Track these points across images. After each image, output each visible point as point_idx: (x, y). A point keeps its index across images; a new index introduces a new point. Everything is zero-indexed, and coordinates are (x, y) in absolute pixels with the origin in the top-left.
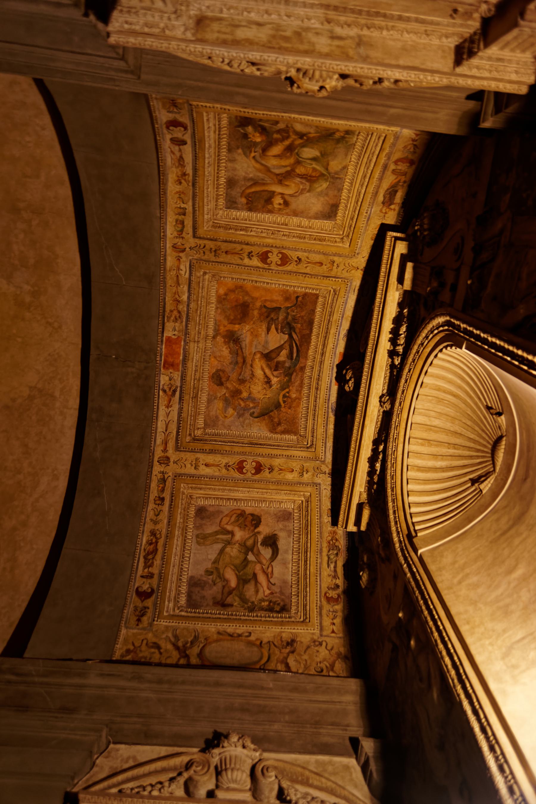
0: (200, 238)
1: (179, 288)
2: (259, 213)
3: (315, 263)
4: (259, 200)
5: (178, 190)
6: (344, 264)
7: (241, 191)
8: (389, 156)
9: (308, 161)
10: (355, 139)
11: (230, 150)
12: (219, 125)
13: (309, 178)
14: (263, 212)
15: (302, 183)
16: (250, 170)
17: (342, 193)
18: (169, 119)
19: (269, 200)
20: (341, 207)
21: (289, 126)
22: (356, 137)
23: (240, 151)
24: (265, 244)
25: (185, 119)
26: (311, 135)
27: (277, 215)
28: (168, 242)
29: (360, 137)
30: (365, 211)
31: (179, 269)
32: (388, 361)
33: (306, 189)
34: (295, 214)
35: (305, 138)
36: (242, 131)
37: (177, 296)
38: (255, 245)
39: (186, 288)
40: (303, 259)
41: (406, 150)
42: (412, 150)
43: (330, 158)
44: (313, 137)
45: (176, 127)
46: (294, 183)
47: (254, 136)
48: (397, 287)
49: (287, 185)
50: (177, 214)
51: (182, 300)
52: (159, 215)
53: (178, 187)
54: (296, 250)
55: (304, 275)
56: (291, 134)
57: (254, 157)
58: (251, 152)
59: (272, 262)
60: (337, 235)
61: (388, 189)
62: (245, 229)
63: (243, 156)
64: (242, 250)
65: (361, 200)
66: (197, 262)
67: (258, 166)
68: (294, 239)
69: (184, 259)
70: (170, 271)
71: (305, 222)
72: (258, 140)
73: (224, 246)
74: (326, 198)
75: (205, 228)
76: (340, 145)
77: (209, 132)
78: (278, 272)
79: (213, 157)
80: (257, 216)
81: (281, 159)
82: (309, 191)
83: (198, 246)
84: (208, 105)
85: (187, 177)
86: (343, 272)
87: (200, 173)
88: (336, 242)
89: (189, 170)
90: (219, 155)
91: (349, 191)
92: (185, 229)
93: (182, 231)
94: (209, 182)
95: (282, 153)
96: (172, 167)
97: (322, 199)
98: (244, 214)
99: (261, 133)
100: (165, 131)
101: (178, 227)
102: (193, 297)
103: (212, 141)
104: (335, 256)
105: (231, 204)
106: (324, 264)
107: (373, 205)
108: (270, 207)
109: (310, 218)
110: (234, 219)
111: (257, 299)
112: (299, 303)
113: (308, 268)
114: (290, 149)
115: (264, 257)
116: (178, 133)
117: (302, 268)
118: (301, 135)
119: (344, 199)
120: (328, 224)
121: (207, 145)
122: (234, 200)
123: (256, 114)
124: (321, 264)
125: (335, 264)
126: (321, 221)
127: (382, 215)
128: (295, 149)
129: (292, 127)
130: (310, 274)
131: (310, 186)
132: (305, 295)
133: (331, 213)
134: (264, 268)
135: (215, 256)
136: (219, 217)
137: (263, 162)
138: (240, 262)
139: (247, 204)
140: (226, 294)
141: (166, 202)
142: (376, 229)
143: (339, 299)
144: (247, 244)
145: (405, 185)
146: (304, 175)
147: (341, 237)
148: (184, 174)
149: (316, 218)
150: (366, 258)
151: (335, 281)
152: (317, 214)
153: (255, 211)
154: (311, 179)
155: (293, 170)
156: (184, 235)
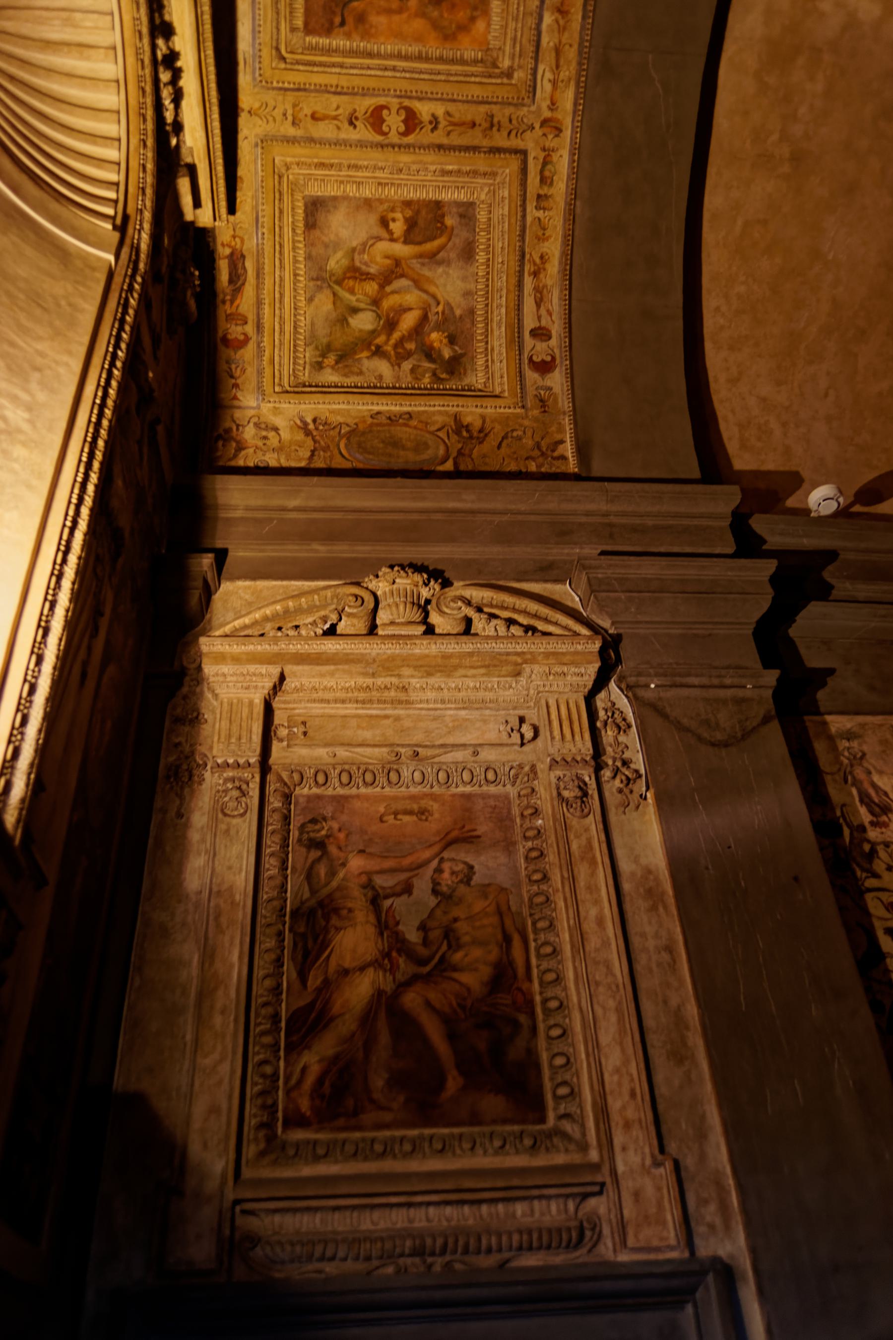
0: (516, 151)
1: (557, 41)
2: (424, 200)
3: (324, 118)
4: (426, 223)
5: (546, 244)
6: (275, 120)
7: (453, 239)
8: (260, 350)
9: (362, 306)
10: (307, 355)
11: (472, 312)
12: (487, 361)
13: (357, 274)
14: (419, 201)
15: (366, 264)
16: (442, 281)
17: (305, 252)
18: (550, 375)
19: (411, 224)
20: (301, 225)
21: (396, 368)
22: (307, 359)
23: (458, 312)
24: (412, 150)
25: (531, 376)
26: (365, 354)
27: (396, 197)
28: (569, 140)
29: (301, 362)
30: (266, 236)
31: (554, 83)
32: (170, 14)
33: (359, 254)
34: (368, 203)
35: (373, 348)
36: (457, 348)
37: (562, 22)
38: (429, 147)
39: (545, 39)
40: (346, 125)
41: (241, 366)
42: (233, 366)
43: (334, 315)
44: (362, 351)
45: (543, 361)
46: (377, 264)
47: (441, 341)
48: (193, 156)
49: (387, 257)
50: (550, 196)
51: (553, 13)
52: (578, 203)
53: (545, 250)
54: (361, 144)
55: (339, 89)
56: (392, 353)
57: (438, 304)
58: (443, 313)
59: (398, 113)
60: (299, 174)
61: (243, 284)
62: (444, 173)
63: (453, 304)
64: (449, 134)
65: (277, 255)
66: (523, 99)
67: (432, 289)
68: (366, 163)
69: (545, 105)
70: (570, 79)
71: (351, 190)
72: (434, 336)
73: (475, 138)
74: (326, 239)
75: (507, 171)
76: (325, 341)
77: (500, 354)
78: (385, 92)
79: (495, 305)
80: (428, 193)
81: (400, 305)
82: (354, 250)
83: (520, 133)
84: (502, 410)
85: (532, 269)
86: (274, 104)
87: (514, 281)
88: (298, 164)
89: (528, 282)
90: (487, 305)
91: (296, 261)
92: (539, 167)
93: (545, 163)
94: (500, 260)
95: (400, 315)
96: (552, 286)
97: (332, 237)
98: (446, 196)
99: (432, 348)
100: (557, 352)
101: (550, 171)
102: (531, 22)
103: (496, 333)
104: (295, 137)
105: (467, 212)
106: (309, 118)
107: (258, 251)
108: (409, 213)
109: (346, 198)
110: (463, 187)
111: (416, 15)
112: (338, 11)
113: (335, 106)
114: (391, 325)
115: (411, 121)
116: (540, 350)
117: (345, 105)
118: (379, 352)
119: (300, 242)
120: (315, 190)
121: (503, 329)
122: (463, 221)
123: (443, 406)
124: (314, 117)
125: (290, 118)
126: (326, 194)
127: (238, 232)
128: (384, 327)
129: (393, 366)
130: (329, 92)
131: (353, 260)
132: (328, 31)
133: (315, 208)
134: (410, 98)
135: (492, 116)
136: (486, 189)
137: (425, 296)
138: (451, 107)
139: (443, 216)
140: (473, 19)
141: (565, 220)
142: (241, 202)
143: (269, 36)
144: (440, 147)
145: (221, 296)
146: (365, 280)
147: (290, 171)
148: (535, 274)
149: (335, 199)
150: (241, 136)
151: (283, 83)
152: (335, 207)
153: (430, 201)
154: (355, 273)
155: (382, 287)
156: (542, 155)
